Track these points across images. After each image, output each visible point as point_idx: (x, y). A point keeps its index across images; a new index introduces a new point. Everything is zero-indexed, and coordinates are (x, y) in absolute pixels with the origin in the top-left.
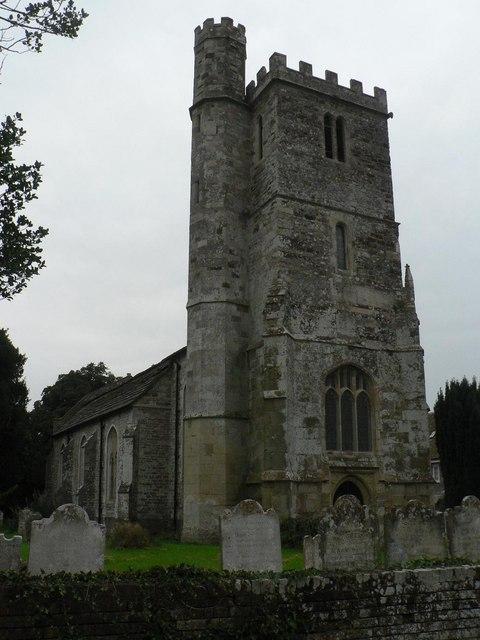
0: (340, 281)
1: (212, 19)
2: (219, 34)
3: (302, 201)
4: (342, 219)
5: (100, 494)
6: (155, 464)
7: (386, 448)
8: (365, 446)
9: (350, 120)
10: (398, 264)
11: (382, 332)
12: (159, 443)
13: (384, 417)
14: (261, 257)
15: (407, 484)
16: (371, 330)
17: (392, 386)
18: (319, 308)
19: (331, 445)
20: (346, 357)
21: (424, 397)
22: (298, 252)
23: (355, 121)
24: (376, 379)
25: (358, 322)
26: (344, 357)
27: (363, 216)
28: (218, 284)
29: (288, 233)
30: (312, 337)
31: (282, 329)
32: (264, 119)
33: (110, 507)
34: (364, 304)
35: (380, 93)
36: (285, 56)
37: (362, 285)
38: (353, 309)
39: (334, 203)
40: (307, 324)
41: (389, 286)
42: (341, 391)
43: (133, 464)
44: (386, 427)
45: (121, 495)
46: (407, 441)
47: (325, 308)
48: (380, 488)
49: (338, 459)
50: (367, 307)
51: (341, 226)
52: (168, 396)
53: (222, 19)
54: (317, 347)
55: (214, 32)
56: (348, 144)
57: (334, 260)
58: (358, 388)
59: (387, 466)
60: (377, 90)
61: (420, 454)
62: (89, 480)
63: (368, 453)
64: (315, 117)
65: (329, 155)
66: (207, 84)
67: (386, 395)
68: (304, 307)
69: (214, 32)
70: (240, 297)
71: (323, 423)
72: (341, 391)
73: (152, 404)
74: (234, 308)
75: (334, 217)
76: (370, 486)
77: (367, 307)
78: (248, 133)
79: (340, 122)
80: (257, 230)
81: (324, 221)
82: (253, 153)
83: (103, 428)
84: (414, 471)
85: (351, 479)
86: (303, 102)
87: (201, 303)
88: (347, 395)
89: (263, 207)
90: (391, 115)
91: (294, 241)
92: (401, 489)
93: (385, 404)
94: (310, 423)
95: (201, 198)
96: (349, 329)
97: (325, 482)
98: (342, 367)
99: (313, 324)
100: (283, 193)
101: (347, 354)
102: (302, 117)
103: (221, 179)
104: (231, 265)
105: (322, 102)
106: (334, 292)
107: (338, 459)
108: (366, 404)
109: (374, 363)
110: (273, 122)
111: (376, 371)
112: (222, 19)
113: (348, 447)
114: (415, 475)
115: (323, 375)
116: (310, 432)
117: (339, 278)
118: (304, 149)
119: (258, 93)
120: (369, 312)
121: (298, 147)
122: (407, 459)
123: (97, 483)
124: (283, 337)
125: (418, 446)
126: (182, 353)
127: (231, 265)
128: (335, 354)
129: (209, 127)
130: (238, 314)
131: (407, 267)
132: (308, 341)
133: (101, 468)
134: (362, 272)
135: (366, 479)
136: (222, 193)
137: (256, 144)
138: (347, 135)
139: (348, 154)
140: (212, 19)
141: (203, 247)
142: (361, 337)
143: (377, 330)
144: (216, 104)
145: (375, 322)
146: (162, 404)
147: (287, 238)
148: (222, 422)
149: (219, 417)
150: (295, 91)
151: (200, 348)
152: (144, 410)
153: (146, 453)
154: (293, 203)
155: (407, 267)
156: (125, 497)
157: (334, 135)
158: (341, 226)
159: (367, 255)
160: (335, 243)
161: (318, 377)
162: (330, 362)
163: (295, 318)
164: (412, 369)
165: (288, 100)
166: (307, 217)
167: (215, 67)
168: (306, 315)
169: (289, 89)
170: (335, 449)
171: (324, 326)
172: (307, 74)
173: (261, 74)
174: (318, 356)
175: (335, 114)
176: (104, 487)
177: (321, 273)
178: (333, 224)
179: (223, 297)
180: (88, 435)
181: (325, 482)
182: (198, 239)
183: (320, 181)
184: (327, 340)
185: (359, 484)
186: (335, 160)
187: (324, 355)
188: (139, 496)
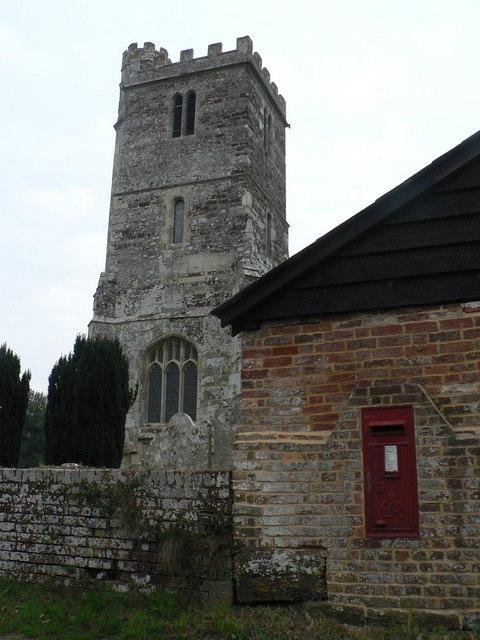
0: (169, 256)
9: (200, 88)
13: (207, 385)
16: (201, 296)
17: (218, 351)
20: (167, 330)
26: (165, 330)
35: (245, 42)
37: (196, 252)
38: (182, 281)
39: (174, 180)
44: (208, 395)
50: (198, 274)
53: (145, 44)
54: (136, 327)
65: (176, 134)
67: (210, 362)
68: (130, 291)
77: (198, 274)
91: (124, 233)
93: (209, 371)
96: (175, 302)
97: (135, 453)
98: (163, 341)
101: (168, 326)
106: (163, 269)
108: (191, 372)
109: (199, 330)
118: (148, 140)
120: (201, 278)
121: (140, 143)
128: (156, 330)
134: (197, 240)
142: (188, 306)
150: (144, 90)
159: (203, 220)
162: (149, 338)
163: (120, 303)
166: (141, 205)
169: (136, 91)
171: (148, 304)
174: (137, 335)
177: (151, 254)
181: (135, 453)
184: (150, 318)
187: (143, 332)
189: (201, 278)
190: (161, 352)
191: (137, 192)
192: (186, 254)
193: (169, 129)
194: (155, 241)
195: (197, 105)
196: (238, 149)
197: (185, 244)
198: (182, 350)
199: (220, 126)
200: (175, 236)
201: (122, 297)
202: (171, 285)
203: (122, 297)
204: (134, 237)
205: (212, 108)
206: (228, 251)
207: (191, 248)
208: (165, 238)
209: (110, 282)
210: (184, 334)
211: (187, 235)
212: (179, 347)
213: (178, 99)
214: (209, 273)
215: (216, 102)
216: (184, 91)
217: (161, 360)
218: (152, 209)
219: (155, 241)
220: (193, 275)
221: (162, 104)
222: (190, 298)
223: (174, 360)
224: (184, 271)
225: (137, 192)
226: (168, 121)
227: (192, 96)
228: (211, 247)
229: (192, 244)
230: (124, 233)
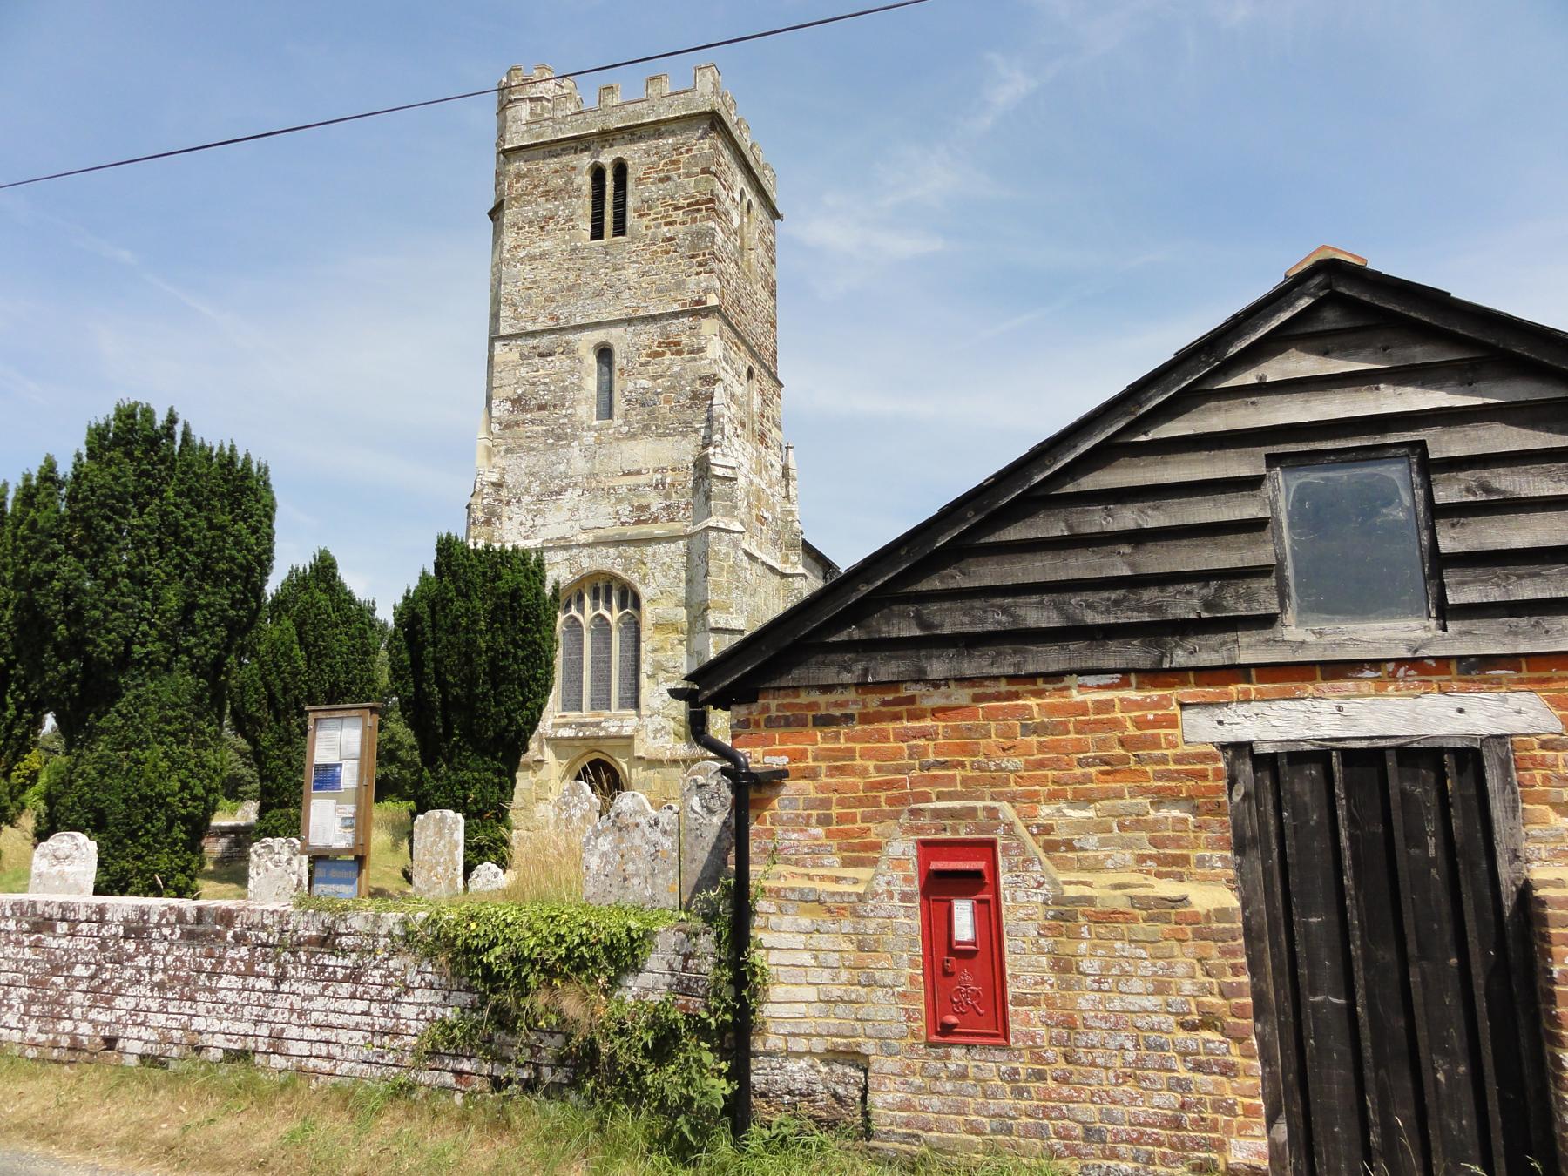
37: (633, 436)
50: (639, 472)
65: (597, 233)
68: (526, 499)
91: (514, 402)
99: (539, 521)
118: (547, 245)
145: (653, 494)
165: (524, 176)
166: (541, 355)
177: (559, 438)
189: (641, 479)
190: (580, 598)
191: (533, 334)
192: (618, 439)
193: (586, 227)
195: (630, 185)
196: (700, 265)
197: (617, 421)
199: (667, 224)
200: (607, 411)
202: (595, 489)
203: (515, 509)
204: (531, 410)
205: (653, 190)
206: (684, 435)
207: (625, 429)
208: (586, 411)
209: (493, 484)
210: (618, 570)
211: (619, 406)
213: (598, 174)
214: (656, 471)
215: (661, 180)
216: (607, 158)
217: (581, 610)
218: (559, 362)
219: (566, 416)
220: (630, 474)
221: (570, 182)
222: (625, 510)
223: (602, 611)
224: (616, 466)
225: (533, 334)
226: (584, 206)
227: (621, 168)
228: (658, 427)
229: (627, 423)
230: (514, 402)
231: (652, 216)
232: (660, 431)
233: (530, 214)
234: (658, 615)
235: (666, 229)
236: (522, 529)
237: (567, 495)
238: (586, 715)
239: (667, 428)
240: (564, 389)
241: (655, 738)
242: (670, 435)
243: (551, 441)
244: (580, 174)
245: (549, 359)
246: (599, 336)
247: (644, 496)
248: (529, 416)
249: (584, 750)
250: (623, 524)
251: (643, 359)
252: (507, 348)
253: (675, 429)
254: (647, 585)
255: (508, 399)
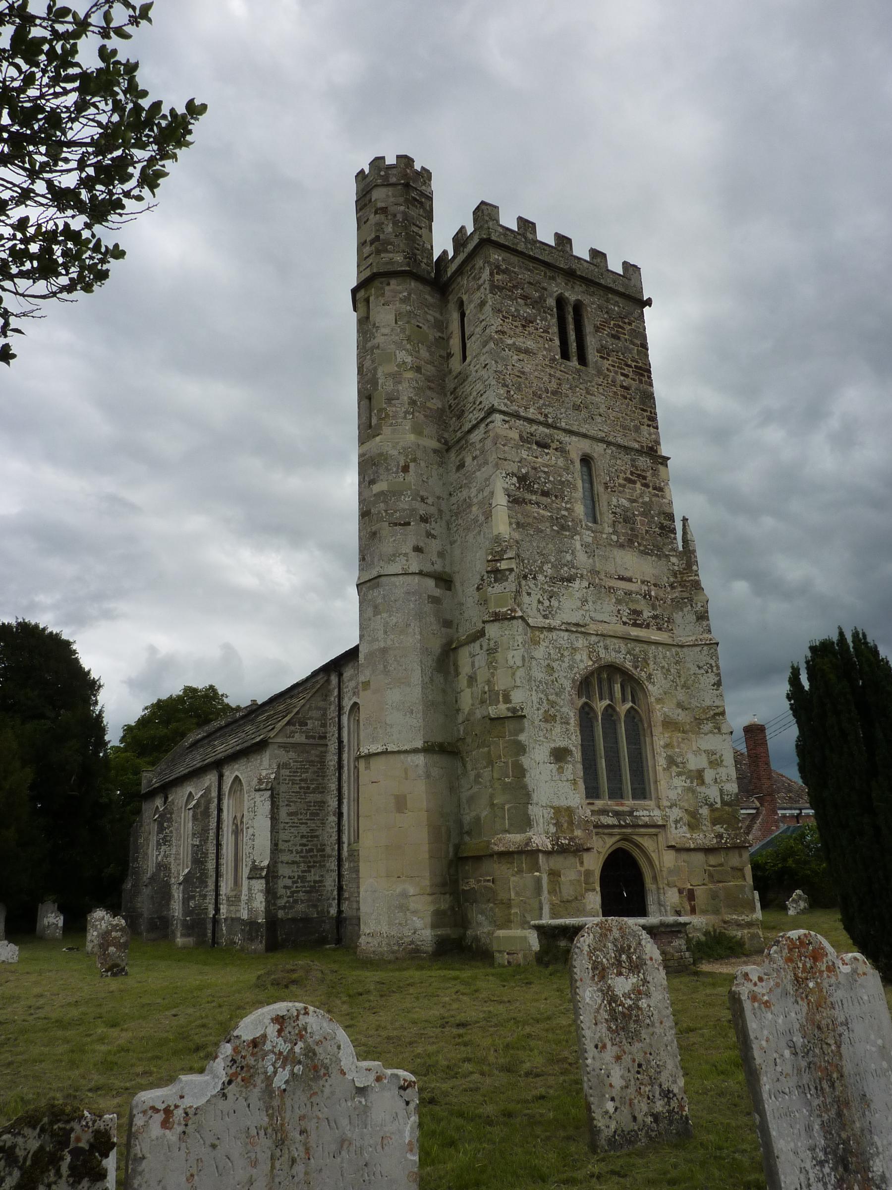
0: (590, 540)
1: (383, 158)
2: (393, 180)
3: (531, 421)
4: (588, 450)
5: (217, 881)
6: (304, 829)
7: (673, 795)
8: (641, 791)
9: (592, 304)
10: (671, 517)
11: (655, 617)
12: (311, 797)
14: (470, 506)
15: (708, 851)
16: (638, 613)
18: (563, 580)
19: (592, 792)
21: (723, 713)
22: (528, 496)
23: (600, 307)
24: (650, 687)
25: (619, 602)
27: (619, 446)
28: (407, 548)
29: (513, 467)
30: (556, 623)
31: (515, 611)
32: (465, 303)
33: (234, 900)
34: (627, 574)
36: (497, 208)
37: (622, 546)
40: (547, 603)
41: (659, 549)
42: (600, 706)
43: (272, 832)
44: (671, 761)
45: (253, 882)
46: (702, 782)
47: (570, 579)
48: (669, 859)
49: (604, 812)
50: (629, 580)
51: (586, 461)
52: (324, 725)
53: (398, 157)
54: (563, 638)
55: (386, 177)
56: (592, 342)
57: (580, 509)
58: (624, 700)
59: (676, 822)
60: (626, 265)
61: (724, 803)
62: (198, 861)
63: (647, 802)
64: (542, 299)
65: (565, 355)
66: (378, 252)
68: (540, 578)
69: (386, 177)
70: (438, 567)
71: (578, 755)
72: (600, 706)
73: (299, 738)
74: (431, 583)
75: (577, 447)
76: (654, 856)
77: (629, 580)
78: (441, 326)
79: (578, 308)
80: (461, 466)
81: (562, 450)
82: (450, 355)
83: (221, 777)
84: (718, 828)
85: (626, 845)
86: (524, 276)
87: (380, 576)
88: (610, 711)
89: (470, 431)
90: (649, 302)
91: (522, 479)
92: (700, 857)
94: (560, 755)
95: (374, 421)
97: (588, 850)
98: (601, 669)
99: (555, 603)
100: (504, 408)
102: (525, 297)
103: (406, 392)
104: (424, 519)
105: (553, 278)
107: (604, 812)
110: (483, 304)
111: (650, 675)
112: (398, 157)
113: (616, 793)
114: (720, 836)
115: (574, 681)
116: (561, 770)
117: (588, 537)
118: (530, 344)
119: (453, 267)
121: (520, 342)
122: (705, 811)
123: (211, 865)
124: (515, 622)
125: (721, 791)
126: (352, 655)
127: (424, 519)
129: (384, 316)
130: (437, 592)
131: (685, 520)
132: (550, 629)
133: (218, 845)
134: (620, 528)
135: (647, 843)
136: (406, 413)
137: (455, 343)
138: (589, 329)
139: (592, 355)
140: (383, 158)
141: (382, 493)
143: (647, 614)
144: (393, 282)
145: (643, 602)
146: (314, 737)
147: (514, 474)
148: (420, 759)
149: (415, 751)
150: (514, 259)
151: (382, 645)
152: (285, 746)
153: (290, 814)
154: (519, 423)
155: (685, 520)
156: (259, 885)
157: (571, 327)
158: (586, 461)
160: (579, 484)
161: (568, 684)
162: (584, 663)
163: (529, 594)
164: (703, 671)
165: (504, 272)
166: (538, 444)
167: (389, 229)
168: (544, 591)
170: (598, 797)
172: (530, 236)
173: (460, 240)
174: (566, 653)
175: (572, 296)
176: (223, 869)
177: (563, 528)
178: (576, 457)
179: (414, 568)
180: (195, 790)
181: (588, 850)
182: (372, 482)
183: (555, 393)
184: (576, 628)
185: (636, 853)
186: (574, 363)
188: (281, 883)
194: (566, 509)
198: (617, 687)
201: (532, 586)
210: (628, 665)
212: (610, 681)
224: (610, 568)
228: (639, 544)
231: (610, 362)
232: (642, 548)
233: (513, 310)
234: (665, 714)
235: (622, 378)
236: (540, 607)
237: (577, 584)
238: (629, 803)
239: (646, 548)
240: (562, 483)
241: (676, 828)
242: (648, 554)
243: (555, 528)
244: (551, 296)
245: (546, 451)
246: (585, 446)
247: (637, 602)
248: (534, 498)
249: (618, 837)
250: (625, 623)
251: (621, 481)
252: (507, 426)
253: (651, 550)
254: (653, 683)
255: (514, 474)
